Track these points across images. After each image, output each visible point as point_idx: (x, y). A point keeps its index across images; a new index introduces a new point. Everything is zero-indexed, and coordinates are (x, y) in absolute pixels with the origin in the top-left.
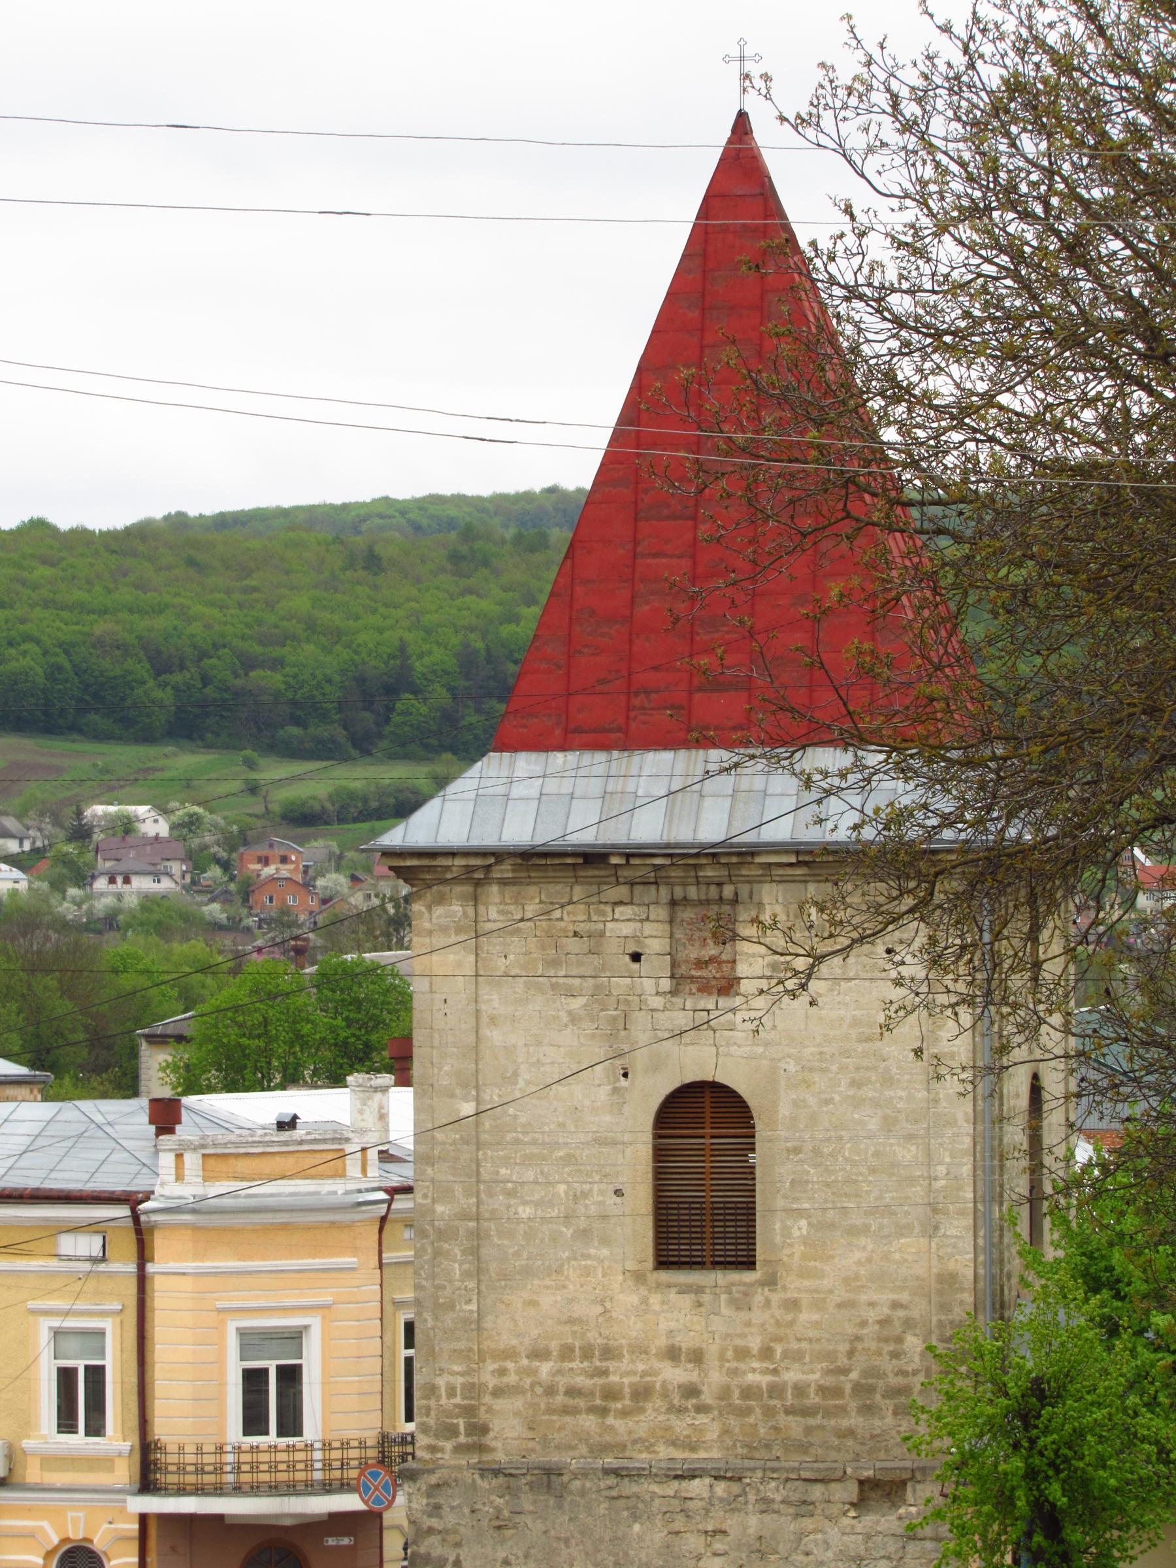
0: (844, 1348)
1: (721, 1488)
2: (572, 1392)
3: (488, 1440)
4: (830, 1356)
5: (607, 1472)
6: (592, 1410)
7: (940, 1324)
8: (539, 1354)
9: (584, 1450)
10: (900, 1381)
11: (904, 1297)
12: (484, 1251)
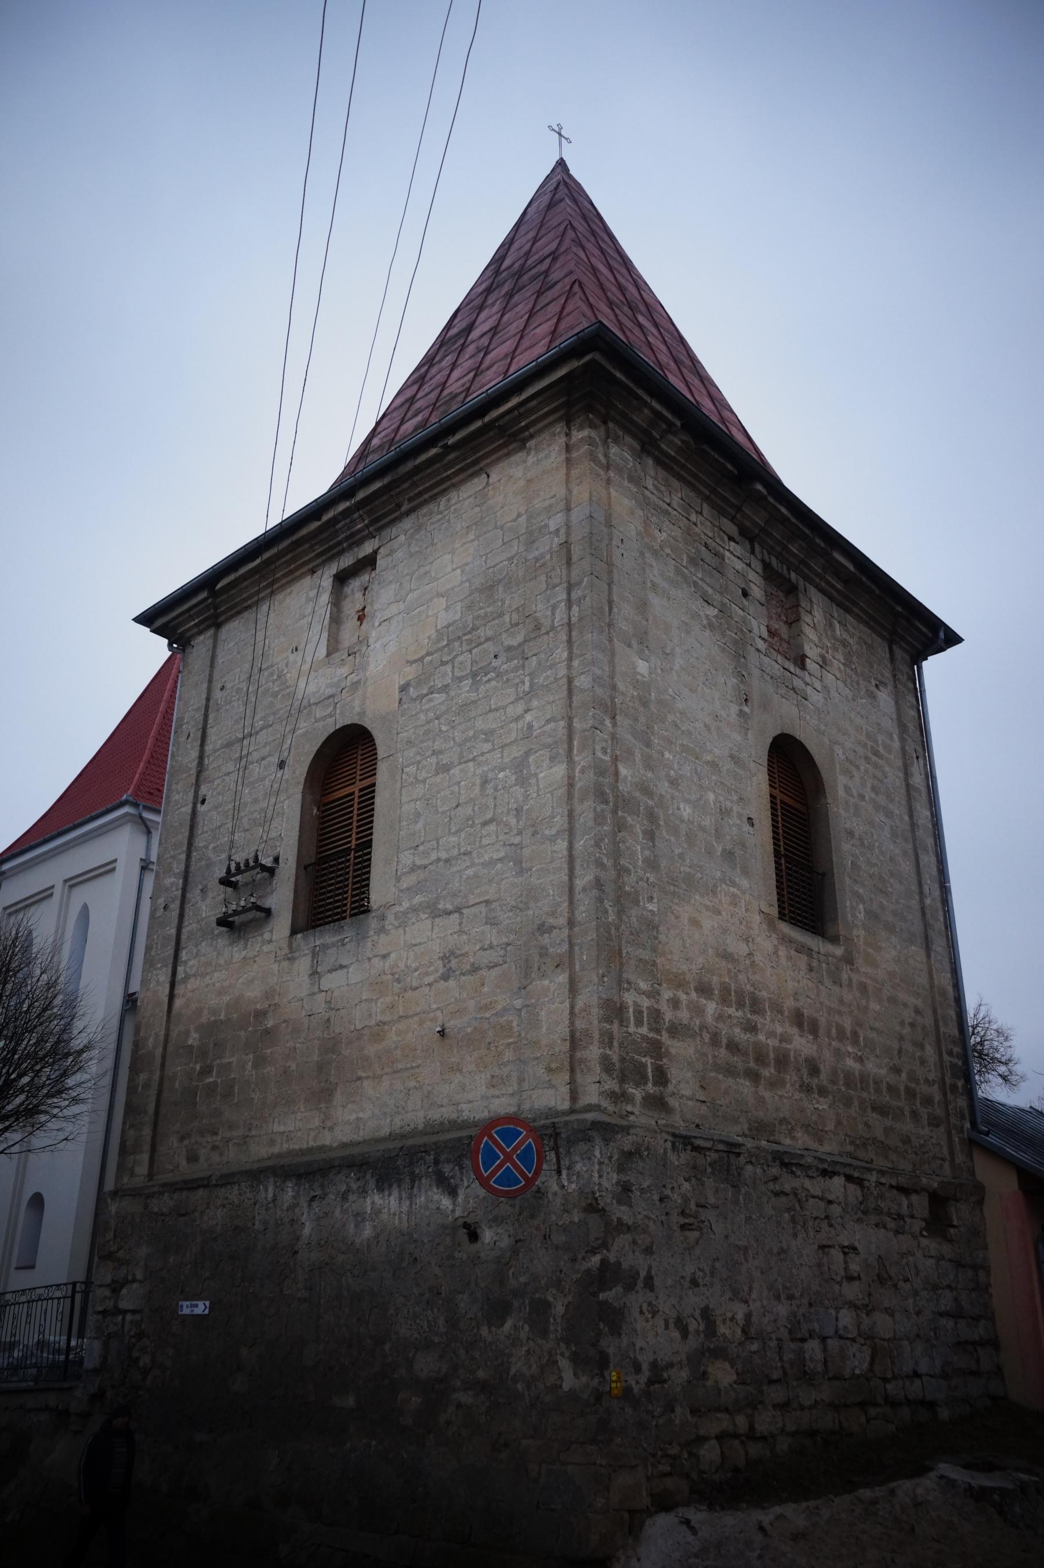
0: (896, 1045)
2: (733, 1047)
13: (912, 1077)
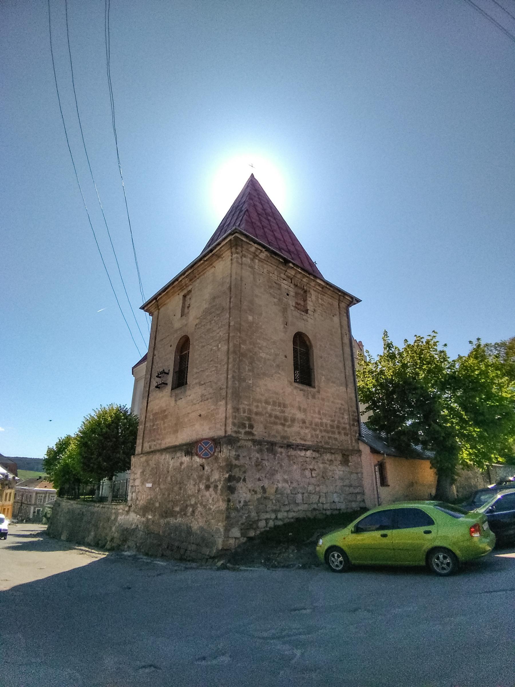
0: (334, 414)
2: (276, 417)
8: (267, 403)
13: (339, 422)
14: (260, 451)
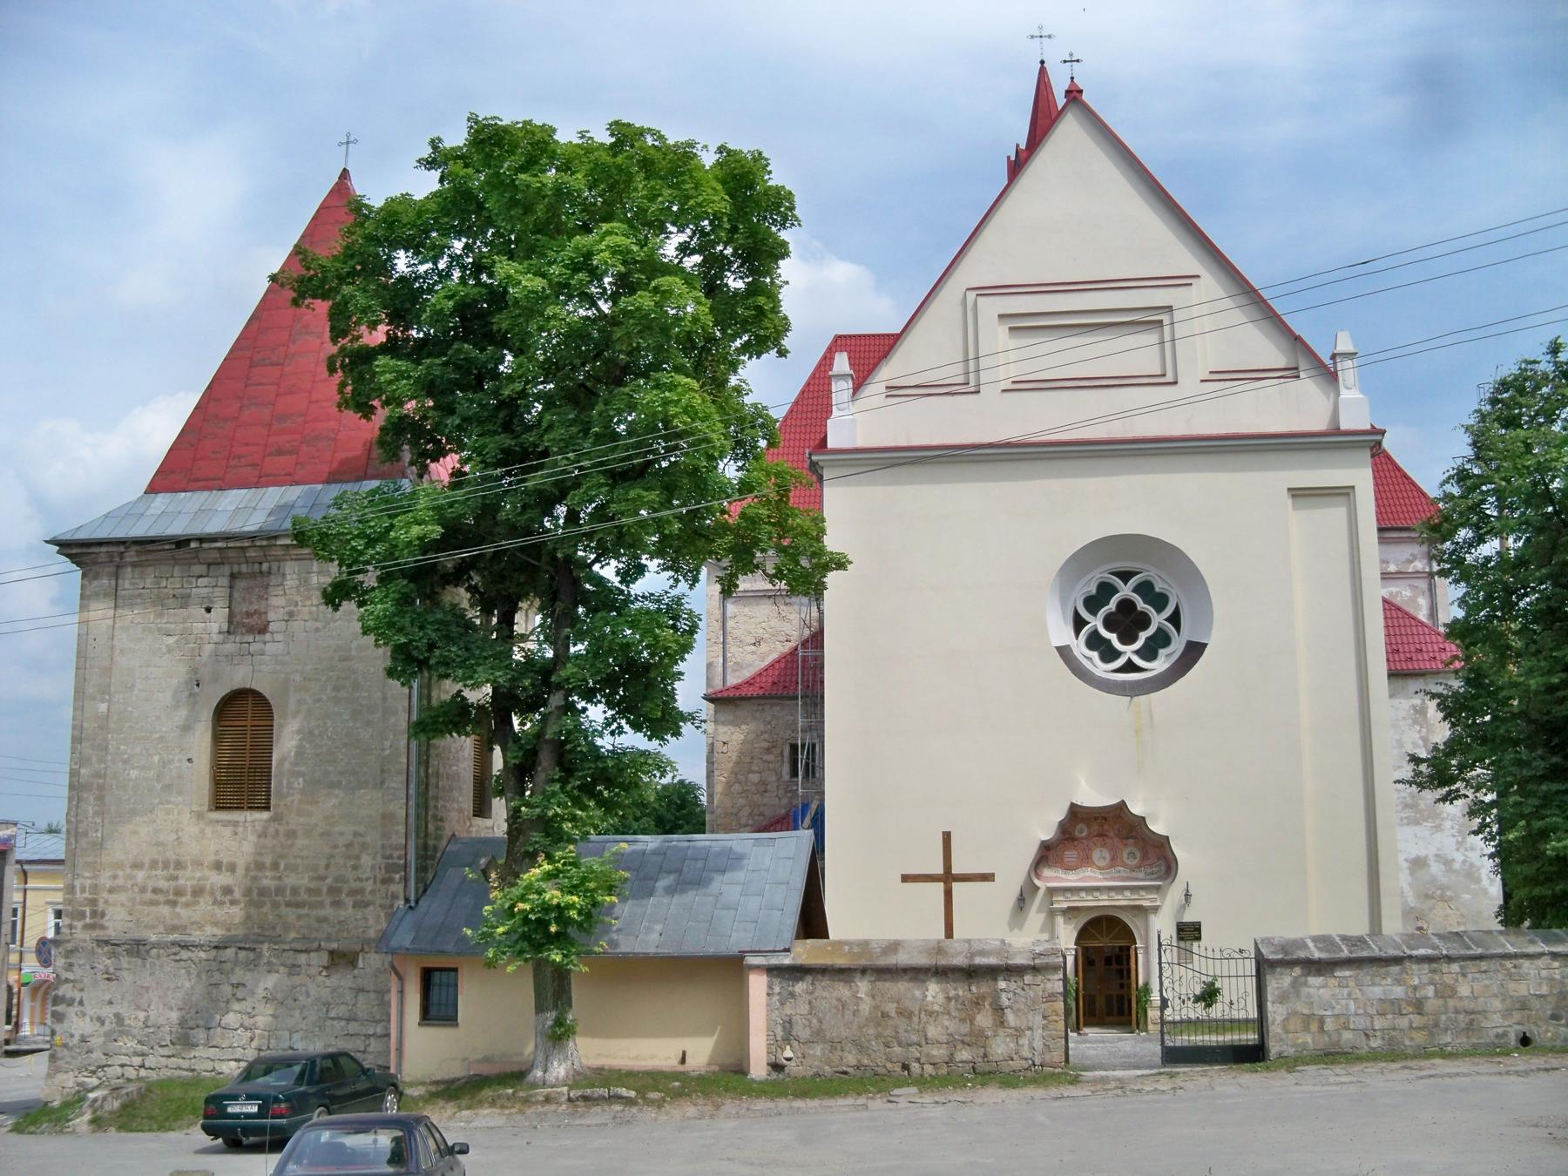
0: (323, 863)
1: (242, 954)
2: (155, 891)
3: (105, 922)
4: (315, 868)
5: (173, 944)
6: (168, 902)
7: (383, 846)
8: (137, 866)
9: (161, 929)
10: (358, 885)
11: (362, 829)
12: (107, 799)
14: (113, 955)
